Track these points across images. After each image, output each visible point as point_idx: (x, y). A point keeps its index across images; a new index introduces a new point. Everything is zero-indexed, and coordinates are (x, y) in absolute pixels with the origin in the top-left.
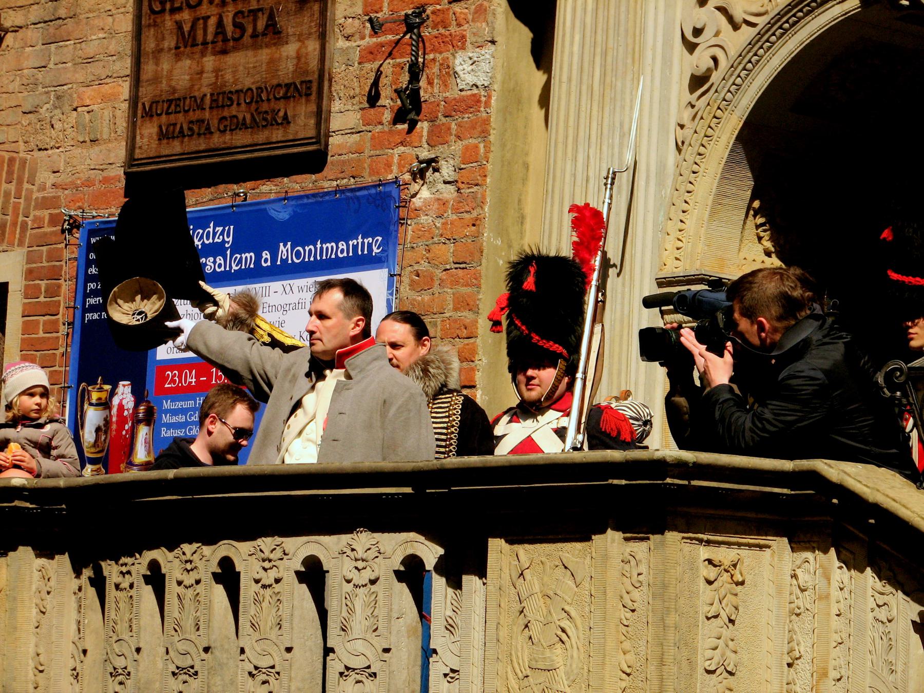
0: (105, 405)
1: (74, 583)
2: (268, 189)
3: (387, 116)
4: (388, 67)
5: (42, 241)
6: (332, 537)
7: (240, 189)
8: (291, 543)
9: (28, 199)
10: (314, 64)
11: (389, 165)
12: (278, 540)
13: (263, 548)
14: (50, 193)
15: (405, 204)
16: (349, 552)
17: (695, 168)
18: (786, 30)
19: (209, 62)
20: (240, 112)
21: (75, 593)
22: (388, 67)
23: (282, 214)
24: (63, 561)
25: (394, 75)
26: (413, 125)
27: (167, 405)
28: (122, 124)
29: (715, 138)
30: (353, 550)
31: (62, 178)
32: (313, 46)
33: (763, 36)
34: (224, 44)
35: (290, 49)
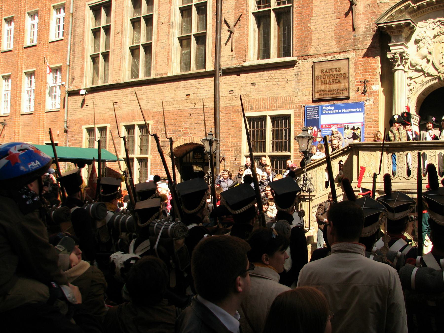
0: (312, 130)
2: (339, 102)
3: (360, 93)
4: (360, 87)
5: (297, 108)
7: (335, 102)
9: (294, 103)
10: (347, 86)
11: (361, 100)
14: (298, 102)
15: (365, 104)
19: (328, 86)
20: (334, 92)
22: (360, 87)
23: (343, 105)
25: (361, 89)
26: (365, 95)
27: (323, 130)
28: (311, 93)
31: (299, 100)
32: (347, 84)
34: (330, 83)
35: (343, 84)
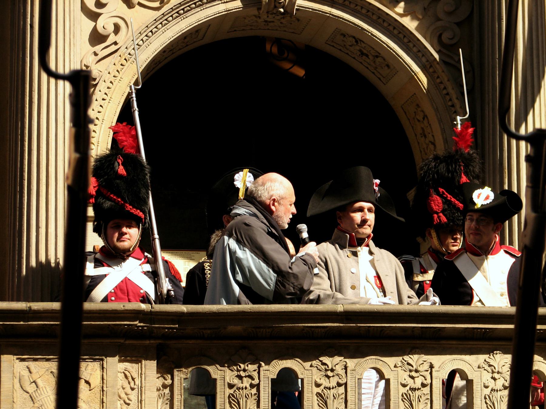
1: (159, 382)
6: (472, 356)
8: (436, 360)
12: (424, 357)
13: (410, 361)
16: (487, 367)
17: (105, 97)
18: (180, 15)
21: (158, 390)
24: (151, 366)
29: (118, 78)
30: (490, 366)
33: (164, 16)
